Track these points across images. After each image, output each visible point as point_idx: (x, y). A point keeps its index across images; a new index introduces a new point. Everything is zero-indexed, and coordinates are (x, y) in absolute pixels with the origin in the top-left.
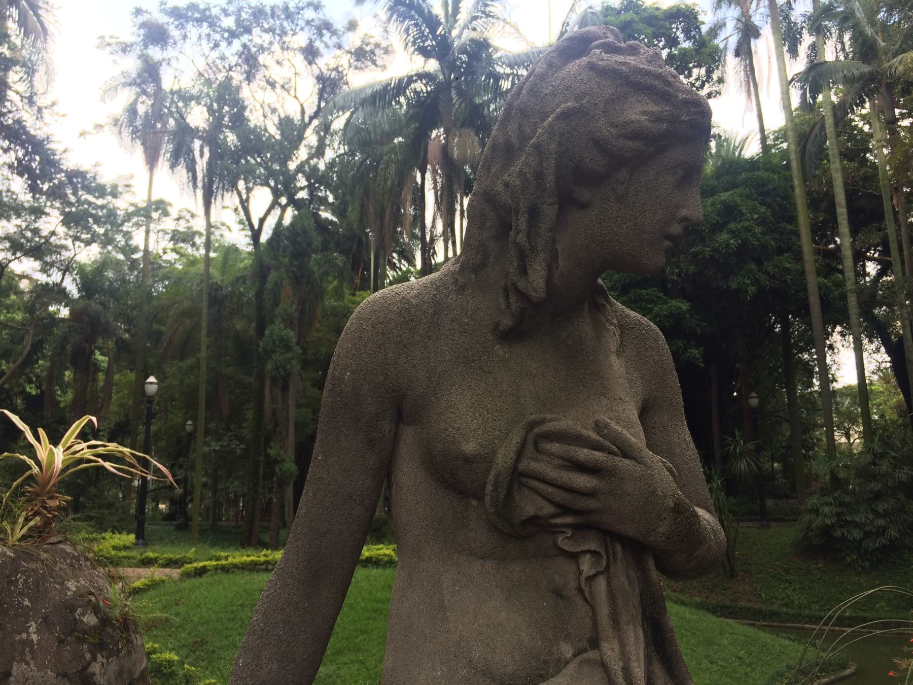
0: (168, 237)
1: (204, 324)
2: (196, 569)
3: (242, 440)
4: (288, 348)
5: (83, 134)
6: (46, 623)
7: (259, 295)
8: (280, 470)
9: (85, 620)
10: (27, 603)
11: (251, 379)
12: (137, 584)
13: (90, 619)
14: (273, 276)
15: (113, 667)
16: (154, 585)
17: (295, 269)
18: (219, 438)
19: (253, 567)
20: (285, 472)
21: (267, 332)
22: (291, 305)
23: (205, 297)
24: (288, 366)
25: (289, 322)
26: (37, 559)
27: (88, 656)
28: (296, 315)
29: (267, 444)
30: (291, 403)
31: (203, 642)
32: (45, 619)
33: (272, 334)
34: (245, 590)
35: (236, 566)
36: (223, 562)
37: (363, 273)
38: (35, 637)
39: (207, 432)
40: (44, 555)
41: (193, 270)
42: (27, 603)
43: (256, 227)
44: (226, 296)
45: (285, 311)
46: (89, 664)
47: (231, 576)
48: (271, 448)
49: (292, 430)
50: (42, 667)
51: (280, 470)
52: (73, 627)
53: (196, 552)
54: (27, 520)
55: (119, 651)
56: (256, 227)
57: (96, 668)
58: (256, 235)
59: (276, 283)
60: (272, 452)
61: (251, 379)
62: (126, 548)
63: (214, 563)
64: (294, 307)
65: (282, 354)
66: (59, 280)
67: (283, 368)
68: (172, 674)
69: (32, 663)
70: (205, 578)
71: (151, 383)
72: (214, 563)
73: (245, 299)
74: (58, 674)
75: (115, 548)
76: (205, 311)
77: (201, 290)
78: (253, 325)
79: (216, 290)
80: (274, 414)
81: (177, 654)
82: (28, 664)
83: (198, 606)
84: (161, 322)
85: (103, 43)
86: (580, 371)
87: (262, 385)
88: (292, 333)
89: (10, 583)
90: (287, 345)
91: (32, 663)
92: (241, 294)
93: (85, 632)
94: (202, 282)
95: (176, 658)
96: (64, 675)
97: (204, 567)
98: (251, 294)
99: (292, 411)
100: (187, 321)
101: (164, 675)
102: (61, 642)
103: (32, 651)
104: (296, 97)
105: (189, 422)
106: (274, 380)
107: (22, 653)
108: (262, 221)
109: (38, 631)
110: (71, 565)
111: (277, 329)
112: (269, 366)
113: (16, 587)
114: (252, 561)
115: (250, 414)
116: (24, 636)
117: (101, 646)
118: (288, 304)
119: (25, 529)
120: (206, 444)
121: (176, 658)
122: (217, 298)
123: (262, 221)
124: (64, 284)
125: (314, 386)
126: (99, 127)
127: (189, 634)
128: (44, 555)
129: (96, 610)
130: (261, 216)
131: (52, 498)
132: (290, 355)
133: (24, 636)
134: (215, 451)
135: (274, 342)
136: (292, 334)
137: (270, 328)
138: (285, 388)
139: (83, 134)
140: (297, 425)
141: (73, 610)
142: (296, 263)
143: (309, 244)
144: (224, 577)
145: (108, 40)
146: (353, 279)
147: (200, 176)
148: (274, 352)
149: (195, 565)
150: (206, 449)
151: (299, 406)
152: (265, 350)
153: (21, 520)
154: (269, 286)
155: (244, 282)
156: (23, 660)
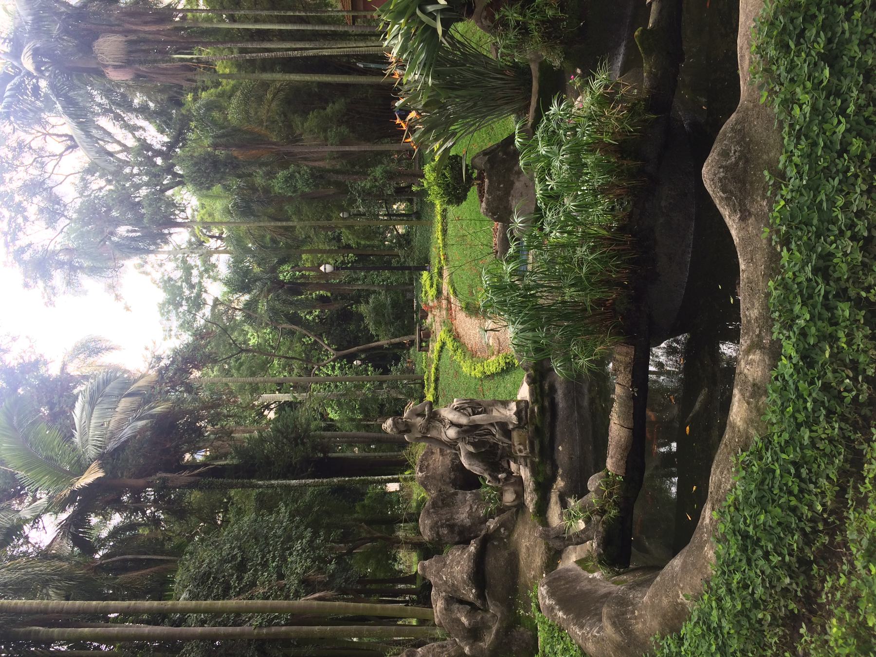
4: (292, 177)
5: (127, 309)
12: (451, 291)
16: (452, 283)
19: (444, 231)
33: (281, 188)
35: (443, 240)
49: (347, 148)
62: (431, 279)
75: (432, 286)
79: (238, 207)
84: (264, 236)
85: (50, 303)
86: (414, 425)
92: (239, 187)
104: (61, 155)
122: (245, 209)
126: (118, 297)
139: (127, 309)
140: (343, 142)
145: (46, 300)
148: (295, 187)
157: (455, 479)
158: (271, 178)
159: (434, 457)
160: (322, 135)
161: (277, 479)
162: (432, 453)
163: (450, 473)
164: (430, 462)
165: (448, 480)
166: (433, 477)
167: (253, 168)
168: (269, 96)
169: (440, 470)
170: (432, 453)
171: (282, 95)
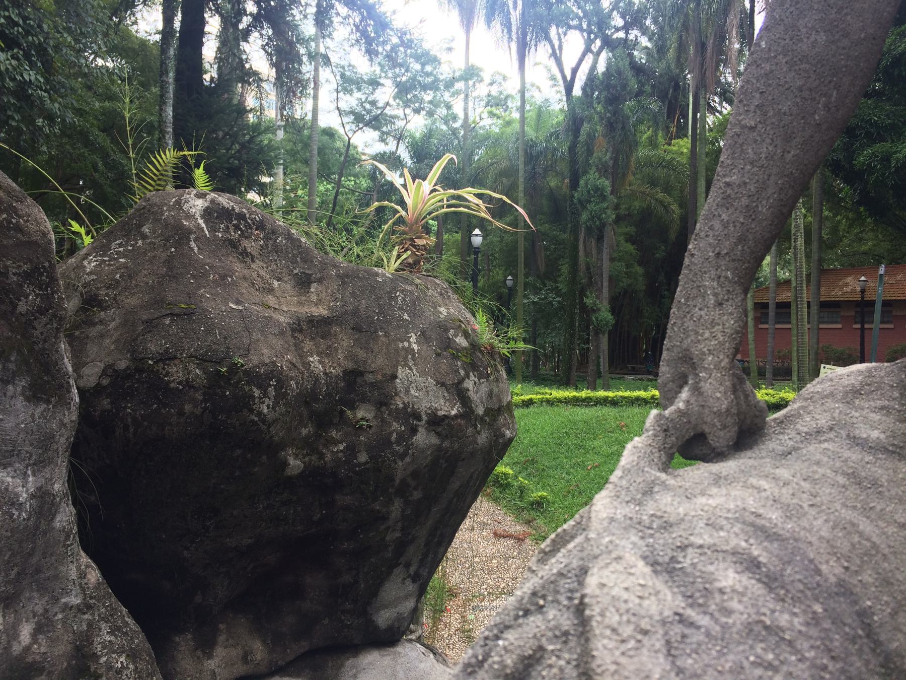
0: (483, 103)
1: (521, 180)
2: (523, 401)
3: (558, 293)
4: (603, 198)
6: (424, 337)
7: (572, 149)
8: (597, 319)
9: (457, 340)
10: (406, 317)
11: (565, 236)
13: (461, 341)
14: (586, 128)
15: (484, 388)
17: (608, 115)
18: (537, 291)
20: (601, 321)
21: (582, 182)
22: (606, 153)
23: (521, 153)
24: (604, 216)
25: (603, 170)
26: (412, 283)
27: (462, 372)
28: (611, 163)
29: (582, 294)
30: (605, 257)
31: (534, 462)
32: (423, 333)
33: (586, 184)
34: (570, 421)
35: (559, 401)
36: (548, 396)
37: (679, 120)
38: (415, 347)
39: (526, 286)
40: (418, 281)
41: (509, 130)
42: (406, 317)
43: (569, 78)
44: (541, 153)
45: (600, 159)
46: (463, 379)
47: (555, 409)
48: (587, 297)
49: (606, 284)
50: (423, 373)
51: (597, 319)
52: (447, 344)
53: (522, 388)
54: (399, 256)
55: (488, 375)
56: (569, 78)
57: (469, 384)
58: (569, 87)
59: (589, 135)
60: (588, 301)
61: (565, 236)
63: (540, 397)
64: (609, 155)
65: (597, 203)
66: (394, 149)
67: (599, 219)
68: (508, 486)
69: (414, 368)
70: (532, 409)
71: (477, 235)
72: (540, 397)
73: (559, 154)
74: (437, 383)
76: (521, 167)
77: (517, 148)
78: (567, 181)
79: (531, 146)
80: (588, 269)
81: (512, 469)
82: (410, 369)
83: (528, 431)
87: (577, 239)
88: (607, 183)
89: (391, 298)
90: (602, 194)
91: (414, 368)
92: (555, 149)
93: (458, 351)
94: (518, 139)
95: (511, 472)
96: (443, 384)
97: (531, 400)
98: (565, 148)
99: (606, 264)
100: (505, 180)
101: (501, 485)
102: (438, 355)
103: (413, 358)
105: (510, 278)
106: (589, 229)
107: (406, 358)
108: (575, 71)
109: (417, 342)
110: (441, 294)
111: (592, 178)
112: (584, 216)
113: (396, 303)
114: (575, 397)
115: (565, 269)
116: (406, 344)
117: (473, 366)
118: (603, 153)
119: (399, 261)
120: (525, 296)
121: (511, 472)
122: (532, 155)
123: (575, 71)
124: (398, 152)
125: (627, 241)
127: (521, 453)
128: (418, 281)
129: (466, 335)
130: (574, 65)
131: (419, 238)
132: (605, 205)
133: (406, 344)
134: (534, 303)
135: (589, 192)
136: (606, 183)
137: (584, 178)
138: (600, 239)
140: (611, 279)
141: (446, 330)
142: (610, 108)
143: (624, 87)
144: (548, 408)
146: (668, 127)
147: (514, 29)
148: (589, 202)
149: (523, 397)
150: (526, 301)
151: (612, 260)
152: (580, 201)
153: (395, 253)
154: (582, 138)
155: (557, 138)
156: (406, 365)
157: (157, 388)
158: (598, 170)
159: (284, 287)
160: (615, 255)
161: (177, 80)
162: (303, 283)
163: (202, 360)
164: (257, 265)
165: (153, 347)
166: (173, 270)
167: (611, 149)
168: (661, 195)
169: (219, 306)
170: (303, 283)
171: (660, 209)
